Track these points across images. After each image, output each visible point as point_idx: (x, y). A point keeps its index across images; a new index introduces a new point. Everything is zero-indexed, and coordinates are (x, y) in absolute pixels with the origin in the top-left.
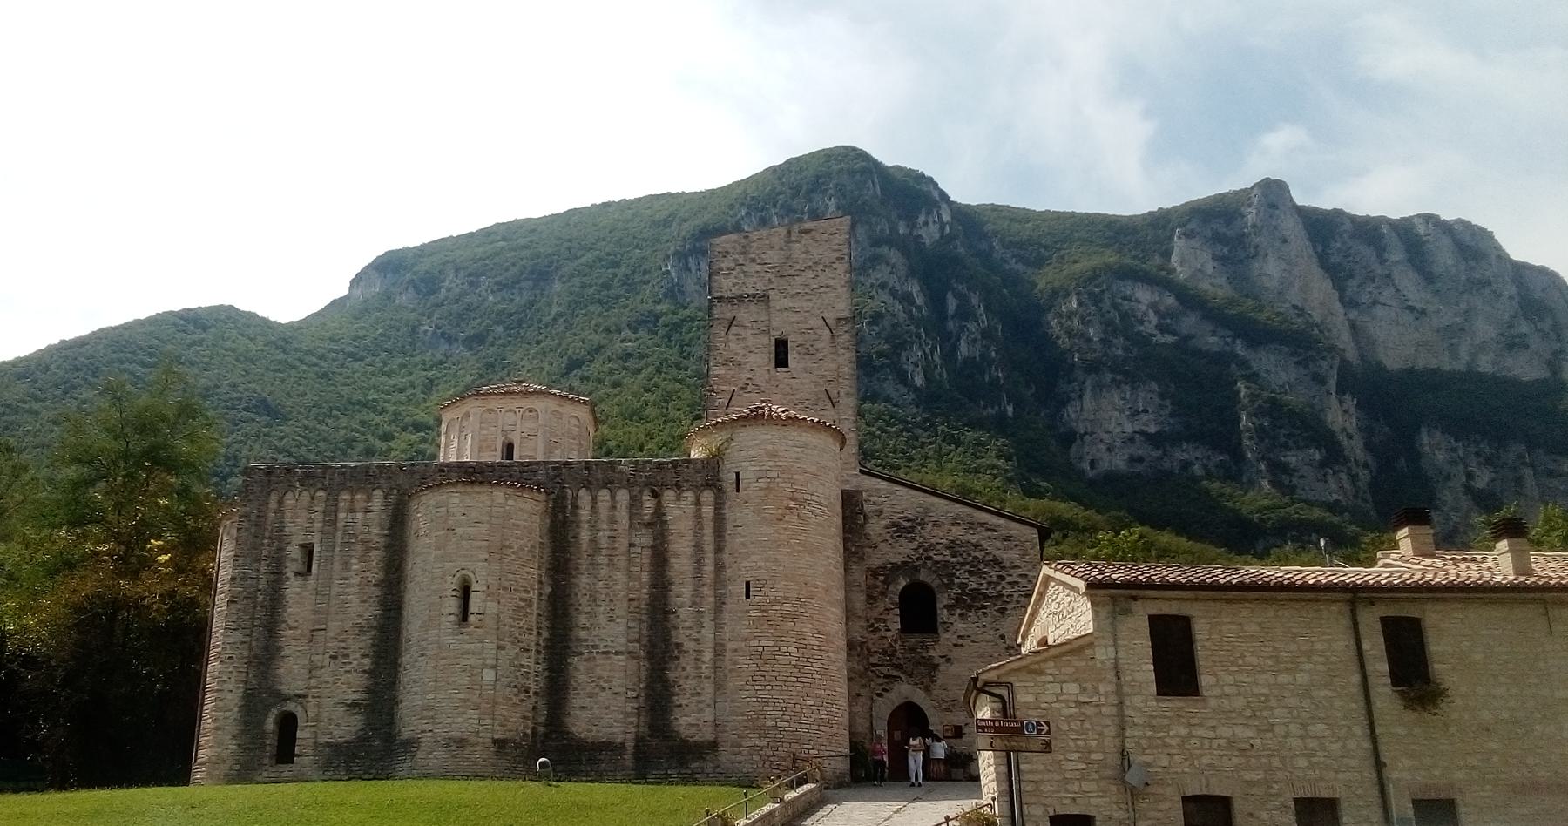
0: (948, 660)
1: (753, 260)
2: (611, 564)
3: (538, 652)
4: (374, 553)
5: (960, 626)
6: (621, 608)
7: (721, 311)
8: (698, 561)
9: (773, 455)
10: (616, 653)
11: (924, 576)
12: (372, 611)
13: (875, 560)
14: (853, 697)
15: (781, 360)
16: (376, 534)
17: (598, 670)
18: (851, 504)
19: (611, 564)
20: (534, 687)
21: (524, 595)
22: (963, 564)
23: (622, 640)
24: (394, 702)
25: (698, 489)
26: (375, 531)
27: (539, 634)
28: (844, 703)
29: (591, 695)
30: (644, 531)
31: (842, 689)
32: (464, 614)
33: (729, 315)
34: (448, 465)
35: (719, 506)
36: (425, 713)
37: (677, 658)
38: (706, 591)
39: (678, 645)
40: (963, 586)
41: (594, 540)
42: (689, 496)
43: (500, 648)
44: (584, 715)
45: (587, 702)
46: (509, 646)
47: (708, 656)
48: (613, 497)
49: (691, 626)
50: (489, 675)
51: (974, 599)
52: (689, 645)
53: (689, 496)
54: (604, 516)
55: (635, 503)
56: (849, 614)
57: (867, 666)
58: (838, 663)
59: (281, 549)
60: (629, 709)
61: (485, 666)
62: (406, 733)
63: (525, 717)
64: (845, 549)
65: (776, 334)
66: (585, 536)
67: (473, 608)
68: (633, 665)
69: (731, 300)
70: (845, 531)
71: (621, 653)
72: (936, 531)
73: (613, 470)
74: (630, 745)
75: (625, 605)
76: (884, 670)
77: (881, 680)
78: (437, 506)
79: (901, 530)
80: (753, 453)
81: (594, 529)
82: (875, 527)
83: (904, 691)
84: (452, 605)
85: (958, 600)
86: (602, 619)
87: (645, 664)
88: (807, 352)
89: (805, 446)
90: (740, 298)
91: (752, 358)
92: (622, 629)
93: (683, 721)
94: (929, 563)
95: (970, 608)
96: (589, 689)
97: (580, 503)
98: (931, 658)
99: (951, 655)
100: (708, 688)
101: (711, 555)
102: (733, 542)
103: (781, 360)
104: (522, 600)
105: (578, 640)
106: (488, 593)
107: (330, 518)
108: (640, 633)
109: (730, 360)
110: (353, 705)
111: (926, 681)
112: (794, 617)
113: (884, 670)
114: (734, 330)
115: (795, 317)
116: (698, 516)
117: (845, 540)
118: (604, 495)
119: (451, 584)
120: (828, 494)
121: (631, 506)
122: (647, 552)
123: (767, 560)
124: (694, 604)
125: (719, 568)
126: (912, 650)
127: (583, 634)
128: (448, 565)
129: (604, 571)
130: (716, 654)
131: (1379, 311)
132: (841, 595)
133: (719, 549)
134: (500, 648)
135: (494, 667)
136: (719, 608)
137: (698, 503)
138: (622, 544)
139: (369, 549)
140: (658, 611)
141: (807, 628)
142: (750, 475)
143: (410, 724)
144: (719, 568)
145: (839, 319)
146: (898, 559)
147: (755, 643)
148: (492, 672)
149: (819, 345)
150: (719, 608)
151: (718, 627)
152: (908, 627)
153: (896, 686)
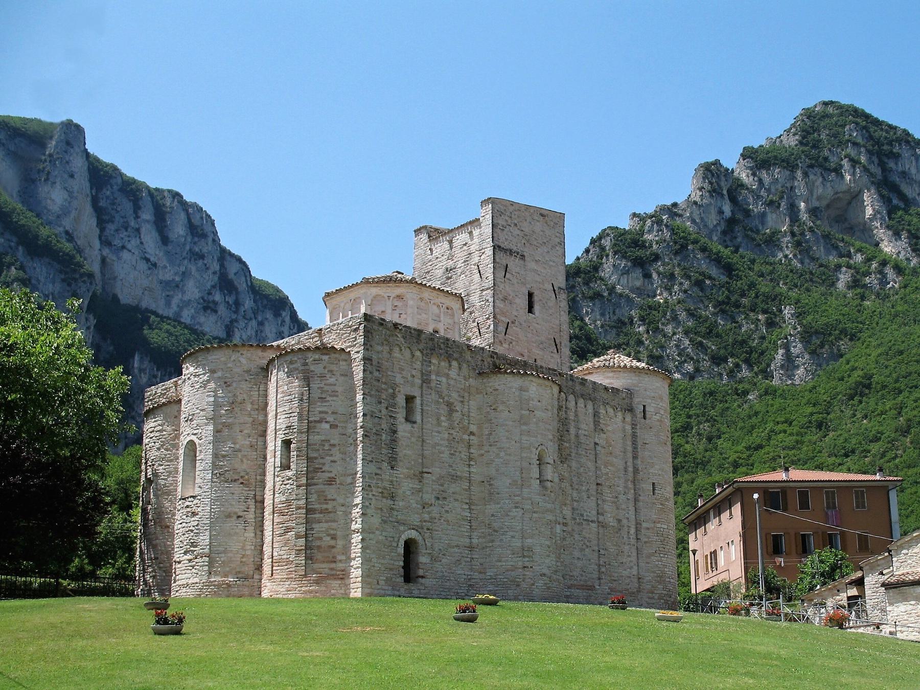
10: (592, 521)
35: (634, 426)
38: (630, 485)
41: (577, 436)
42: (620, 414)
47: (633, 531)
59: (393, 396)
75: (595, 487)
80: (653, 394)
101: (631, 460)
107: (426, 381)
131: (125, 255)
144: (636, 471)
147: (659, 525)
150: (636, 500)
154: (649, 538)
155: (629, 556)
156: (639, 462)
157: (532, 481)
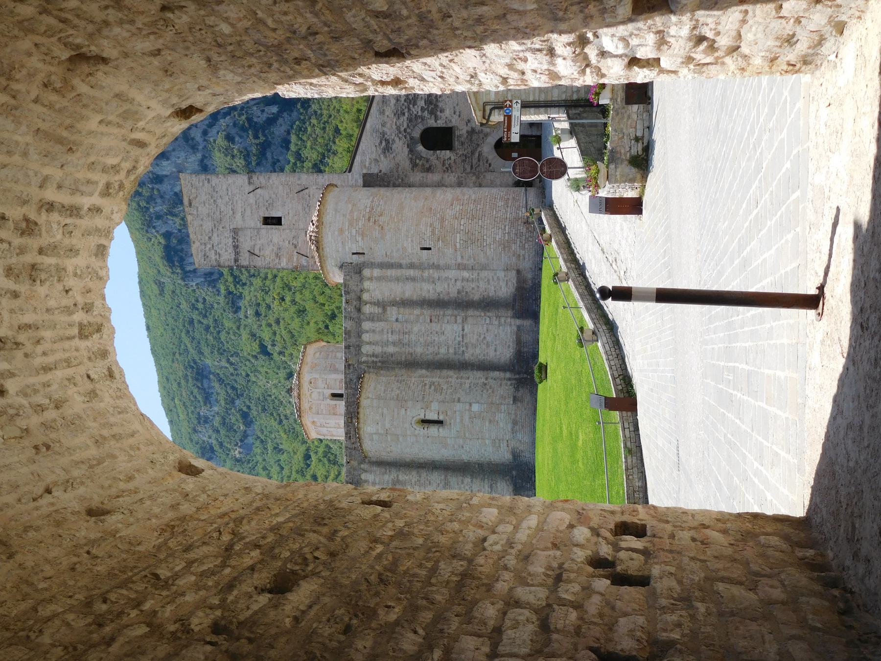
0: (469, 121)
1: (210, 238)
2: (409, 333)
3: (461, 378)
4: (401, 478)
5: (448, 112)
6: (435, 327)
7: (244, 260)
8: (407, 279)
9: (341, 231)
10: (463, 330)
11: (417, 134)
12: (436, 477)
13: (407, 164)
14: (492, 185)
15: (278, 221)
16: (389, 477)
17: (474, 341)
18: (370, 181)
19: (409, 333)
20: (483, 380)
21: (427, 387)
22: (409, 109)
23: (455, 327)
24: (490, 464)
25: (361, 280)
26: (386, 477)
27: (451, 377)
28: (494, 191)
29: (488, 345)
30: (388, 312)
31: (485, 191)
32: (440, 422)
33: (247, 255)
34: (346, 434)
35: (372, 265)
36: (497, 445)
37: (467, 292)
38: (426, 274)
39: (459, 292)
40: (423, 109)
41: (394, 344)
42: (367, 284)
43: (459, 401)
44: (499, 348)
45: (493, 348)
46: (458, 395)
47: (466, 274)
48: (367, 332)
49: (447, 285)
50: (475, 407)
51: (431, 103)
52: (459, 284)
53: (367, 284)
54: (377, 338)
55: (372, 318)
56: (440, 185)
57: (474, 173)
58: (469, 193)
60: (497, 323)
61: (470, 410)
62: (511, 457)
63: (501, 385)
64: (399, 186)
65: (259, 224)
66: (391, 349)
67: (435, 418)
68: (470, 320)
69: (237, 254)
70: (388, 186)
71: (463, 327)
72: (388, 125)
73: (349, 331)
74: (518, 322)
75: (433, 324)
76: (475, 161)
77: (481, 163)
78: (372, 440)
79: (387, 148)
80: (340, 244)
81: (387, 343)
82: (385, 165)
83: (487, 149)
84: (433, 430)
85: (432, 113)
86: (443, 338)
87: (470, 312)
88: (271, 205)
89: (336, 210)
90: (236, 247)
91: (275, 240)
92: (449, 327)
93: (504, 289)
94: (408, 130)
95: (436, 106)
96: (484, 347)
97: (370, 353)
98: (468, 132)
99: (466, 119)
100: (484, 274)
101: (404, 271)
102: (395, 258)
103: (278, 221)
104: (430, 388)
105: (455, 354)
106: (427, 407)
108: (452, 315)
109: (277, 255)
110: (491, 487)
111: (481, 136)
112: (442, 220)
113: (475, 161)
114: (257, 252)
115: (248, 212)
116: (379, 279)
117: (395, 186)
118: (366, 337)
119: (421, 431)
120: (365, 197)
121: (373, 320)
122: (402, 310)
123: (407, 236)
124: (433, 282)
125: (412, 266)
126: (462, 144)
127: (451, 351)
128: (409, 433)
129: (413, 337)
130: (465, 269)
132: (428, 190)
133: (400, 266)
134: (459, 401)
135: (471, 405)
136: (437, 267)
137: (371, 279)
138: (397, 326)
139: (398, 481)
140: (439, 304)
141: (449, 213)
142: (354, 246)
143: (503, 455)
144: (412, 266)
145: (249, 183)
146: (406, 150)
147: (458, 245)
148: (473, 405)
149: (267, 197)
150: (437, 267)
151: (448, 267)
152: (449, 146)
153: (485, 154)
154: (470, 257)
155: (488, 280)
156: (403, 262)
157: (441, 435)
